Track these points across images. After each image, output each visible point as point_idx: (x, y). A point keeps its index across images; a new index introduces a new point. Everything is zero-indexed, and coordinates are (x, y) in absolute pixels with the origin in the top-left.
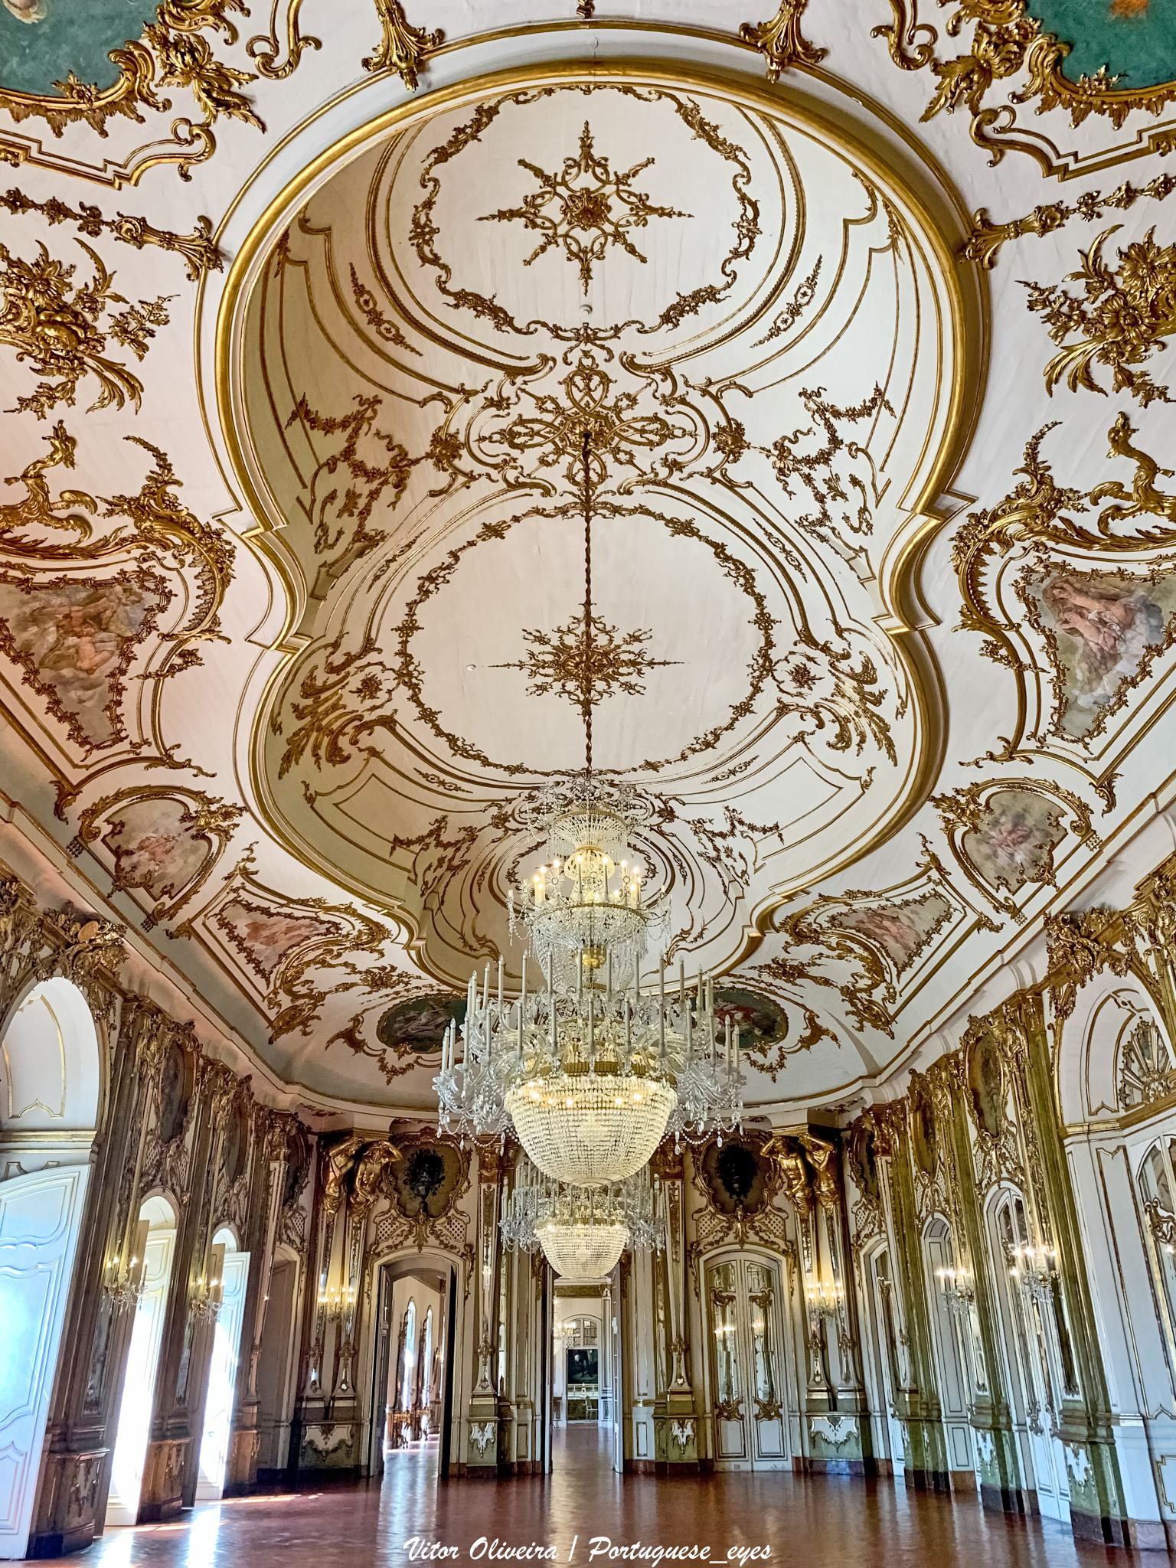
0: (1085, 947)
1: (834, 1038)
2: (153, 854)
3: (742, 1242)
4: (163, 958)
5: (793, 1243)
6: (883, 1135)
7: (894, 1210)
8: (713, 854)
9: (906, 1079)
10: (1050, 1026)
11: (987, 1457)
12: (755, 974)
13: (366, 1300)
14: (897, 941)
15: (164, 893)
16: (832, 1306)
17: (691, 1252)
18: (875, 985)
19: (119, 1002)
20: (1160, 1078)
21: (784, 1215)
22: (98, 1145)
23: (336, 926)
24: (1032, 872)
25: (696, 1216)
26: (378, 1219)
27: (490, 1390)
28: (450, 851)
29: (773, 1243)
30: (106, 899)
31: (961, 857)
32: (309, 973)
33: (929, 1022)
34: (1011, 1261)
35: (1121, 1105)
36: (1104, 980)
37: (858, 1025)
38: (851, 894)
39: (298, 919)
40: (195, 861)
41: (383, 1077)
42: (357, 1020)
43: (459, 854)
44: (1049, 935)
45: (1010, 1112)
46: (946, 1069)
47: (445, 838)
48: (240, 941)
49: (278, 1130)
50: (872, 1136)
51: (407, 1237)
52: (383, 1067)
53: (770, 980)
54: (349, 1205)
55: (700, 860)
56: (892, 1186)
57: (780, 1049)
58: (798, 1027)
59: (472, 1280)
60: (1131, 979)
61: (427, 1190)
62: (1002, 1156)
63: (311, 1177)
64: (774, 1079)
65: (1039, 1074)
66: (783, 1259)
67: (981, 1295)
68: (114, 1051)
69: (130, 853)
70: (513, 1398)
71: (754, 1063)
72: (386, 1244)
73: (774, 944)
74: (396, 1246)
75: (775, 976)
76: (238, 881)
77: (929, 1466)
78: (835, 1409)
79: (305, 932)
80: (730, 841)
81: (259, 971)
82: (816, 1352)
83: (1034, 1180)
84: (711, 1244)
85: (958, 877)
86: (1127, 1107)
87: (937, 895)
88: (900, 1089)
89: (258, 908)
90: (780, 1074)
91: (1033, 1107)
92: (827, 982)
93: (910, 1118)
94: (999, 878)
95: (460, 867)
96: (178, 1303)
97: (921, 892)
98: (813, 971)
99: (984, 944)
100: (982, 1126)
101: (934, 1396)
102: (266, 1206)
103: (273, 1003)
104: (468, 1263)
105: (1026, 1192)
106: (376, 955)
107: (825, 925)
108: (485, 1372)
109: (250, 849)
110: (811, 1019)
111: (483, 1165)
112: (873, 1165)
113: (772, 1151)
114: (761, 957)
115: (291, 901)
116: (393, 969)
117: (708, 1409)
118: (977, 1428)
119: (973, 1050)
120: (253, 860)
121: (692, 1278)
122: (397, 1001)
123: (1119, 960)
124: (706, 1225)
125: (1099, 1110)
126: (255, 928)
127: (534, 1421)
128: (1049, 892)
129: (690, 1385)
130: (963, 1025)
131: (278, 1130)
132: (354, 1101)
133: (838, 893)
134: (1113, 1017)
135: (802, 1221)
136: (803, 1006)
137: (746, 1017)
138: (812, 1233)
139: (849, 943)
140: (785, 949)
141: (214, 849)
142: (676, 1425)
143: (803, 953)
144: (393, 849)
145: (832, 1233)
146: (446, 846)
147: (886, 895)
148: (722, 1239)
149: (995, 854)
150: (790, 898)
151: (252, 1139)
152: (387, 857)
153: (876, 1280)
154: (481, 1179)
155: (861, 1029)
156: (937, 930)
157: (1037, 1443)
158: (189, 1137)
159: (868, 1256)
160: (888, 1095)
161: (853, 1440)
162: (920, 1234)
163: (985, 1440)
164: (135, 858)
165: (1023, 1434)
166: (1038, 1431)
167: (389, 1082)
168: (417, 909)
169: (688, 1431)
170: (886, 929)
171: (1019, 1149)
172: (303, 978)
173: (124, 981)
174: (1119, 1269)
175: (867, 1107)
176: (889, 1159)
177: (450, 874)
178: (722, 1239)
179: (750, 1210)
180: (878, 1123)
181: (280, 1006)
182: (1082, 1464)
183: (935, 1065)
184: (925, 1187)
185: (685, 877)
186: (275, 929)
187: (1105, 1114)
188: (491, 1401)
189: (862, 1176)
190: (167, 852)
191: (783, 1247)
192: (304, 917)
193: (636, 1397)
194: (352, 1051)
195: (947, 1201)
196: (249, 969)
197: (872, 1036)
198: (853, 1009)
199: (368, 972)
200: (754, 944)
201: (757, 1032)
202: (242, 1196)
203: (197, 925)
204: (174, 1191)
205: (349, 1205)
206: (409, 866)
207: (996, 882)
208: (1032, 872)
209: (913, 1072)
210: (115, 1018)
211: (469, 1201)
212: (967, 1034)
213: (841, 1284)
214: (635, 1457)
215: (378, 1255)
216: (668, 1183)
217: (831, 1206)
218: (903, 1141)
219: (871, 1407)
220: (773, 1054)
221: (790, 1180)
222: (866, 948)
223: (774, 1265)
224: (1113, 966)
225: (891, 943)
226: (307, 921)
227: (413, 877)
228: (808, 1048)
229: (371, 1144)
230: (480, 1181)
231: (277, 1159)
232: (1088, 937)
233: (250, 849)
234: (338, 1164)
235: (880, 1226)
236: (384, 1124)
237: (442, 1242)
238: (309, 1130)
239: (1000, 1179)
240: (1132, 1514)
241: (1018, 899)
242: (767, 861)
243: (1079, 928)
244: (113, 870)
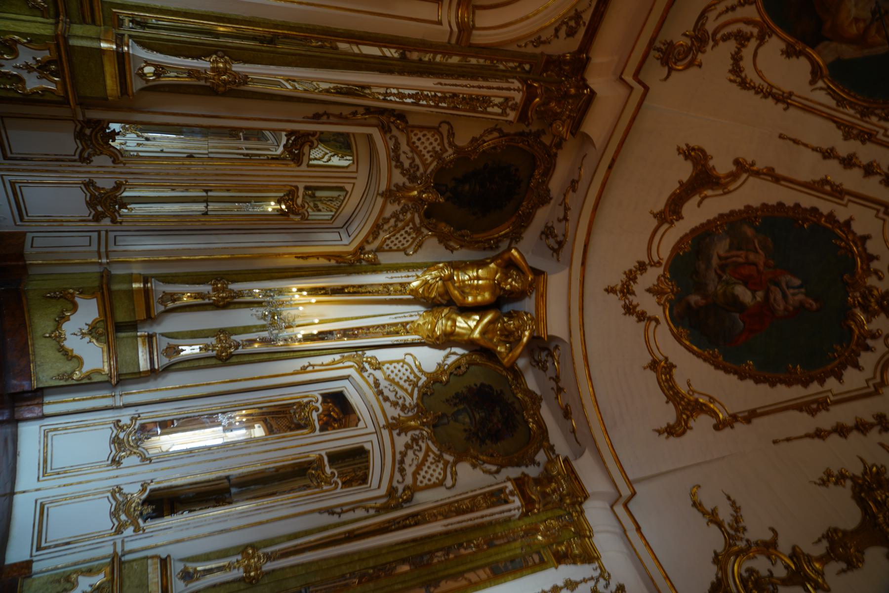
1: (671, 431)
25: (445, 129)
29: (375, 238)
64: (610, 290)
71: (642, 267)
90: (616, 302)
137: (736, 304)
142: (43, 55)
148: (400, 165)
161: (68, 367)
169: (33, 83)
178: (400, 165)
179: (431, 214)
191: (368, 248)
216: (518, 97)
220: (649, 304)
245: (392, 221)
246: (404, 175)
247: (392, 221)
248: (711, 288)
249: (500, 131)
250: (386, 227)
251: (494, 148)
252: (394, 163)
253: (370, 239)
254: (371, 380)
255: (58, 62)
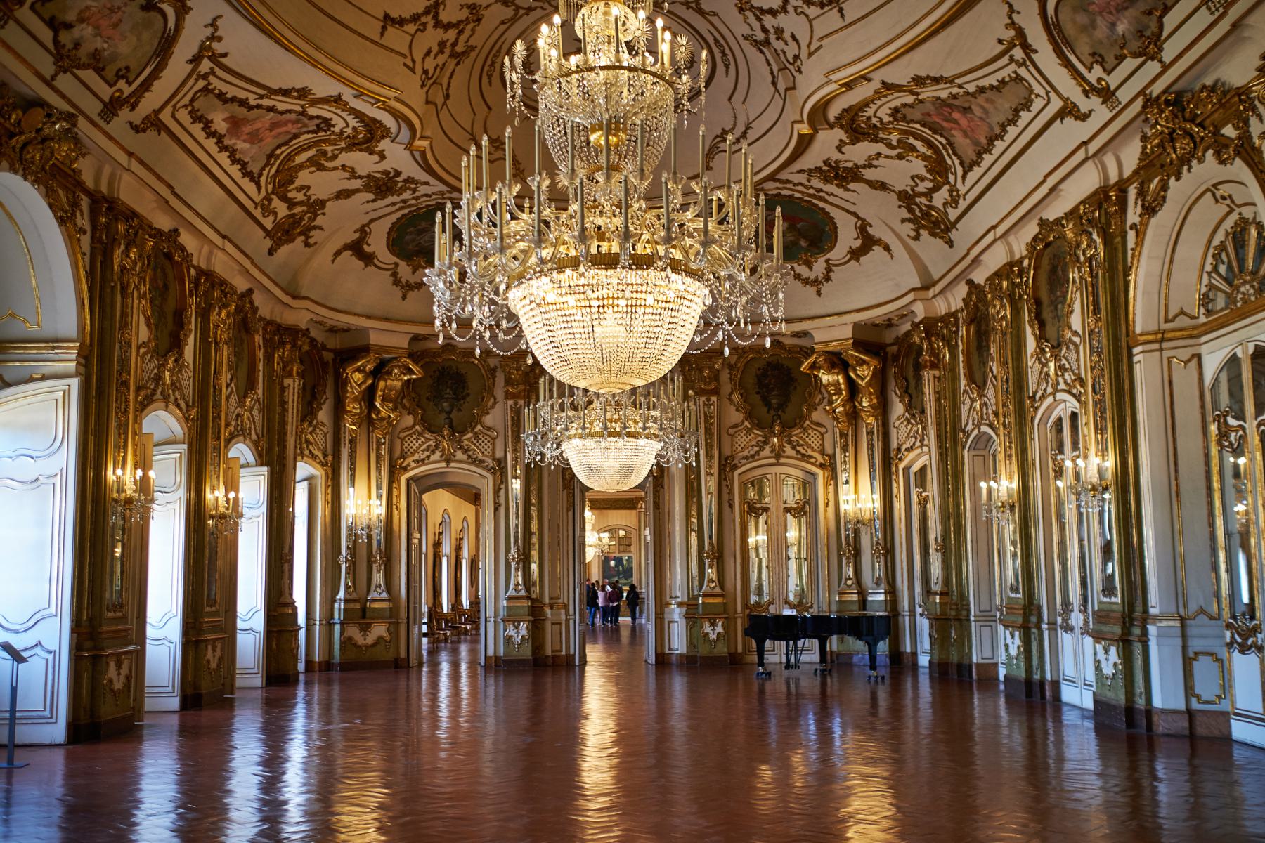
0: (1189, 134)
1: (887, 248)
2: (97, 27)
3: (778, 456)
4: (131, 154)
5: (832, 457)
6: (933, 348)
7: (938, 424)
8: (760, 36)
9: (962, 290)
10: (1133, 226)
11: (1013, 652)
12: (802, 178)
13: (395, 512)
14: (965, 134)
15: (119, 76)
16: (867, 516)
17: (726, 466)
18: (936, 189)
19: (85, 203)
20: (1253, 280)
21: (823, 430)
22: (84, 357)
23: (327, 122)
24: (1135, 45)
25: (731, 431)
26: (402, 435)
27: (523, 593)
28: (451, 35)
29: (811, 457)
30: (49, 83)
31: (1053, 30)
32: (304, 177)
33: (994, 227)
34: (1059, 473)
35: (1202, 310)
36: (1207, 169)
37: (913, 234)
38: (919, 81)
39: (282, 113)
40: (150, 41)
41: (398, 292)
42: (364, 231)
43: (463, 38)
44: (1146, 120)
45: (1076, 321)
46: (1008, 278)
47: (444, 17)
48: (220, 139)
49: (288, 346)
50: (919, 350)
51: (433, 452)
52: (397, 282)
53: (820, 185)
54: (370, 421)
55: (746, 45)
56: (938, 400)
57: (827, 261)
58: (847, 238)
59: (502, 493)
60: (1239, 169)
61: (452, 406)
62: (1061, 368)
63: (329, 393)
64: (819, 294)
65: (1112, 280)
66: (819, 472)
67: (1022, 504)
68: (87, 258)
69: (68, 26)
70: (547, 600)
71: (798, 277)
72: (412, 459)
73: (827, 143)
74: (423, 460)
75: (827, 180)
76: (206, 66)
77: (954, 657)
78: (864, 609)
79: (293, 129)
80: (782, 20)
81: (247, 174)
82: (848, 558)
83: (1094, 391)
84: (746, 458)
85: (1046, 56)
86: (1209, 312)
87: (1018, 79)
88: (956, 299)
89: (233, 99)
90: (826, 288)
91: (1103, 314)
92: (882, 186)
93: (963, 331)
94: (1093, 54)
95: (464, 54)
96: (196, 514)
97: (999, 76)
98: (869, 174)
99: (1070, 133)
100: (1040, 338)
101: (964, 598)
102: (283, 423)
103: (267, 210)
104: (498, 476)
105: (1083, 404)
106: (376, 158)
107: (886, 119)
108: (516, 577)
109: (213, 24)
110: (863, 228)
111: (509, 382)
112: (919, 378)
113: (814, 366)
114: (811, 159)
115: (272, 92)
116: (398, 173)
117: (739, 609)
118: (1006, 627)
119: (1040, 255)
120: (220, 39)
121: (725, 491)
122: (406, 211)
123: (1227, 146)
124: (742, 439)
125: (1175, 317)
126: (235, 124)
127: (567, 621)
128: (1153, 67)
129: (722, 587)
130: (1032, 229)
131: (288, 346)
132: (369, 317)
133: (903, 80)
134: (1209, 211)
135: (842, 435)
136: (855, 214)
138: (851, 448)
139: (911, 140)
140: (839, 148)
141: (171, 23)
142: (707, 624)
143: (860, 152)
144: (384, 28)
145: (871, 446)
146: (447, 27)
147: (958, 81)
148: (757, 453)
149: (1093, 25)
150: (849, 86)
151: (260, 354)
152: (376, 38)
153: (914, 491)
154: (508, 396)
155: (917, 238)
156: (1013, 121)
157: (1066, 640)
158: (189, 352)
159: (907, 470)
160: (941, 307)
162: (964, 447)
163: (1013, 636)
164: (76, 32)
165: (1052, 632)
166: (1069, 629)
167: (404, 297)
168: (418, 102)
169: (719, 629)
170: (956, 122)
171: (1081, 360)
172: (298, 183)
173: (88, 179)
174: (1176, 479)
175: (917, 320)
176: (937, 373)
177: (454, 62)
178: (757, 453)
179: (788, 426)
180: (928, 337)
181: (275, 214)
182: (1111, 660)
183: (996, 274)
184: (973, 400)
185: (727, 66)
186: (258, 125)
187: (1183, 321)
188: (526, 603)
189: (906, 391)
190: (115, 26)
192: (289, 111)
193: (668, 599)
194: (362, 264)
195: (996, 414)
196: (235, 170)
197: (929, 246)
198: (908, 216)
199: (368, 176)
200: (804, 143)
201: (803, 243)
202: (255, 412)
203: (165, 116)
204: (178, 406)
205: (370, 421)
206: (405, 51)
207: (1089, 60)
208: (1135, 45)
209: (970, 283)
210: (83, 221)
211: (495, 417)
212: (1035, 239)
213: (877, 496)
214: (667, 651)
215: (405, 469)
216: (703, 399)
217: (871, 420)
218: (954, 356)
219: (900, 608)
220: (819, 266)
221: (830, 395)
222: (930, 145)
223: (810, 478)
224: (1218, 154)
225: (958, 138)
226: (293, 116)
227: (411, 65)
228: (858, 260)
229: (390, 360)
230: (506, 398)
231: (290, 375)
232: (1192, 121)
233: (213, 24)
234: (356, 379)
235: (922, 441)
236: (403, 342)
237: (469, 456)
238: (324, 347)
239: (1056, 391)
240: (1157, 702)
241: (1113, 81)
242: (823, 43)
243: (1184, 110)
244: (51, 47)
245: (798, 448)
246: (764, 449)
247: (798, 448)
248: (792, 238)
249: (731, 394)
250: (803, 452)
251: (741, 395)
252: (757, 457)
253: (813, 460)
254: (906, 453)
255: (709, 619)
